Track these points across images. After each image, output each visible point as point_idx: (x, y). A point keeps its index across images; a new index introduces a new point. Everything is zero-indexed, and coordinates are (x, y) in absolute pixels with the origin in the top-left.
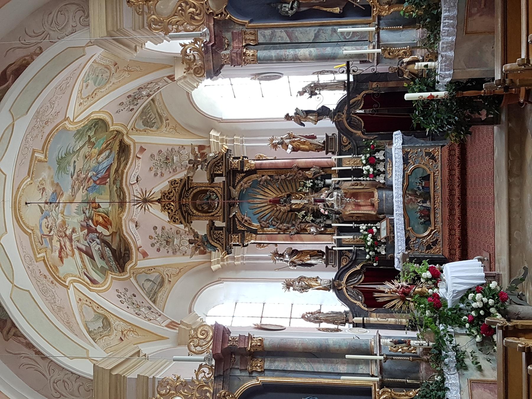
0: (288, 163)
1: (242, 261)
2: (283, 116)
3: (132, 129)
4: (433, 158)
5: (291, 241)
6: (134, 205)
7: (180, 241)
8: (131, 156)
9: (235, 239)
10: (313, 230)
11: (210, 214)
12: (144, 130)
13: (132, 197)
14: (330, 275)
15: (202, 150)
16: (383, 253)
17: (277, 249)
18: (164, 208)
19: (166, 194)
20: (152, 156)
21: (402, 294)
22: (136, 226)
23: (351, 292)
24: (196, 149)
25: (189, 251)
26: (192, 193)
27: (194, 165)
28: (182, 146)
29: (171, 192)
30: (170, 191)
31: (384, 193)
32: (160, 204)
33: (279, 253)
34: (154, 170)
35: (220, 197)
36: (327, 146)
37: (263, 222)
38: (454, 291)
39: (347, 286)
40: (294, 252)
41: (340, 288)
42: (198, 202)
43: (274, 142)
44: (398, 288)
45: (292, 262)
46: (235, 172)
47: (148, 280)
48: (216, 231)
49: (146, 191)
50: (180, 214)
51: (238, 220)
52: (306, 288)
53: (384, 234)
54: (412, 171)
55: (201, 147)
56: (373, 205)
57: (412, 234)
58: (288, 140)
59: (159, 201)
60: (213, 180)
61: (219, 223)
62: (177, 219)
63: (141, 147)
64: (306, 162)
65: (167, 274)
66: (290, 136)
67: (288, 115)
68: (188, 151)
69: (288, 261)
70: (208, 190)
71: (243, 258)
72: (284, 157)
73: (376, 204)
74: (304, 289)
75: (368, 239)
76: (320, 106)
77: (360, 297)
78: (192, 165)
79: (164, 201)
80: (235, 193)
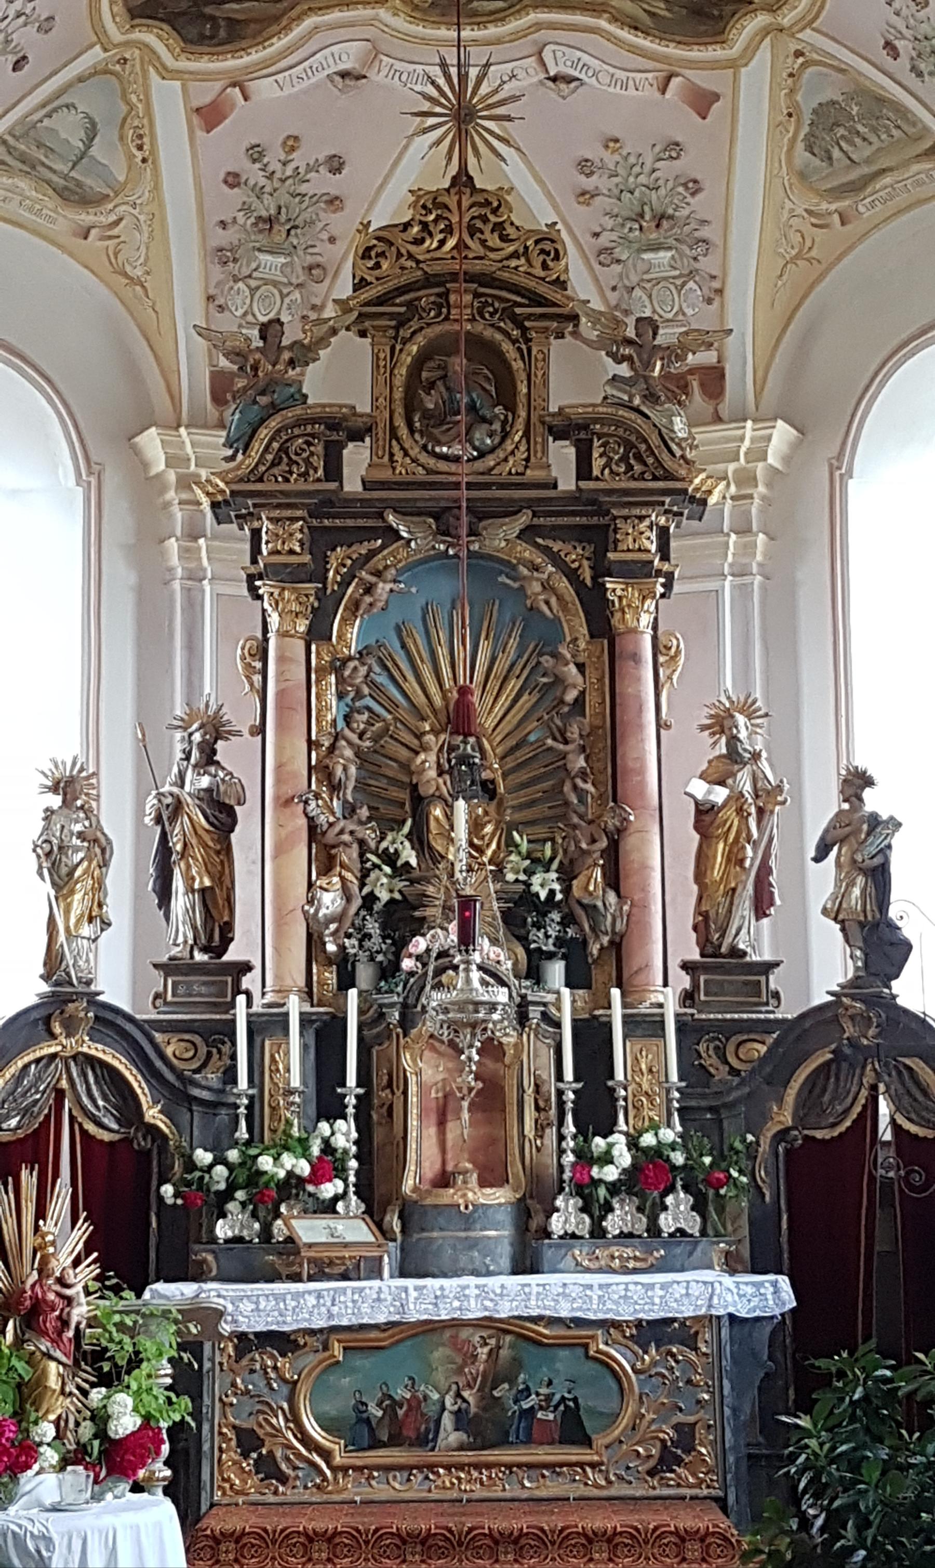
0: (643, 784)
1: (179, 572)
2: (861, 761)
3: (798, 54)
4: (668, 1460)
5: (277, 798)
6: (444, 65)
7: (275, 284)
8: (672, 50)
9: (287, 539)
10: (330, 901)
11: (400, 422)
12: (797, 106)
13: (477, 56)
14: (116, 977)
15: (702, 385)
16: (223, 1230)
17: (238, 734)
18: (430, 204)
19: (495, 211)
20: (674, 149)
21: (34, 1297)
22: (344, 75)
23: (39, 1079)
24: (707, 357)
25: (226, 323)
26: (498, 337)
27: (629, 342)
28: (720, 292)
29: (504, 238)
30: (510, 230)
31: (500, 1235)
33: (220, 745)
34: (611, 160)
35: (479, 465)
36: (721, 966)
37: (363, 670)
38: (48, 1540)
39: (66, 1060)
40: (221, 813)
41: (57, 1029)
42: (458, 364)
43: (741, 719)
44: (61, 1281)
45: (177, 807)
46: (599, 537)
47: (92, 133)
48: (319, 449)
49: (508, 118)
50: (403, 280)
51: (372, 553)
52: (54, 868)
53: (310, 1230)
54: (605, 1364)
55: (713, 381)
56: (444, 1180)
57: (309, 1360)
58: (748, 788)
59: (462, 181)
60: (559, 434)
62: (378, 266)
63: (716, 97)
64: (645, 867)
65: (117, 223)
66: (767, 797)
67: (868, 782)
68: (698, 315)
69: (182, 786)
70: (511, 408)
71: (194, 576)
72: (669, 770)
73: (448, 1196)
74: (55, 863)
75: (288, 1160)
76: (908, 931)
77: (13, 1122)
78: (631, 333)
79: (466, 205)
80: (501, 537)
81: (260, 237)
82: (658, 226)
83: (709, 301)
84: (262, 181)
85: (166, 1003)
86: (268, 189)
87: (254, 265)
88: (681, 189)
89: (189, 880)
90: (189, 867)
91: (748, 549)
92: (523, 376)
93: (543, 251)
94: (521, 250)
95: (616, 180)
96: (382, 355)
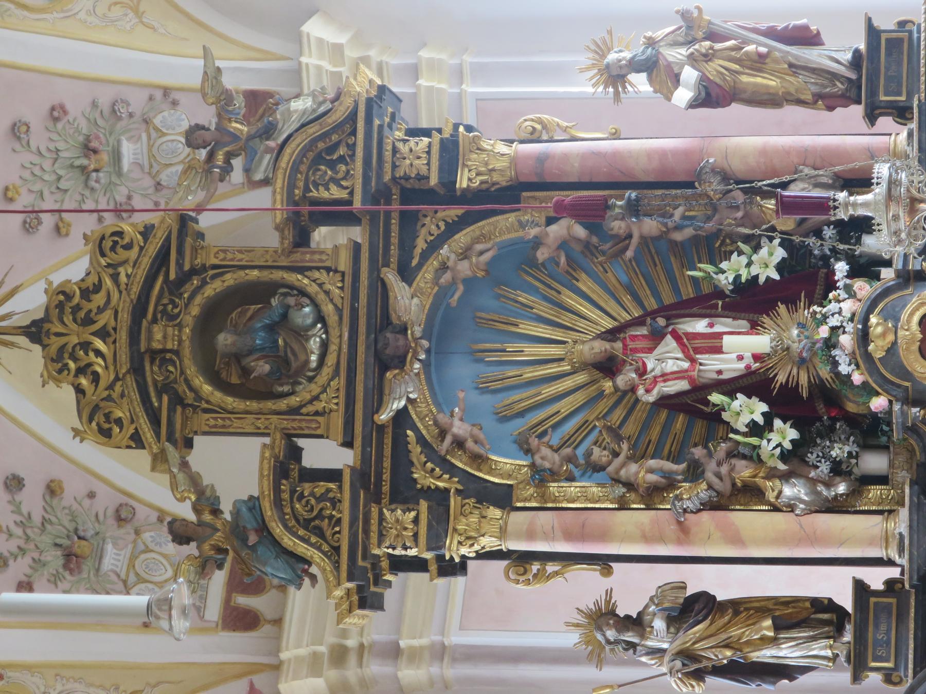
0: (675, 153)
1: (435, 670)
5: (679, 542)
10: (793, 490)
11: (283, 404)
17: (609, 593)
18: (58, 364)
19: (69, 297)
26: (199, 300)
27: (211, 156)
28: (166, 91)
29: (97, 288)
32: (37, 348)
33: (621, 612)
35: (332, 319)
37: (545, 451)
40: (693, 608)
42: (225, 340)
43: (612, 57)
45: (687, 655)
48: (307, 488)
50: (136, 396)
51: (421, 440)
58: (684, 51)
60: (302, 240)
61: (324, 453)
62: (119, 422)
64: (763, 152)
69: (664, 651)
70: (271, 288)
71: (440, 652)
78: (203, 153)
80: (409, 302)
81: (85, 568)
82: (95, 151)
83: (175, 103)
84: (27, 560)
85: (896, 668)
86: (36, 555)
87: (114, 577)
88: (60, 126)
89: (765, 642)
90: (748, 643)
91: (435, 66)
92: (241, 273)
93: (113, 249)
94: (111, 271)
95: (46, 193)
96: (212, 422)
